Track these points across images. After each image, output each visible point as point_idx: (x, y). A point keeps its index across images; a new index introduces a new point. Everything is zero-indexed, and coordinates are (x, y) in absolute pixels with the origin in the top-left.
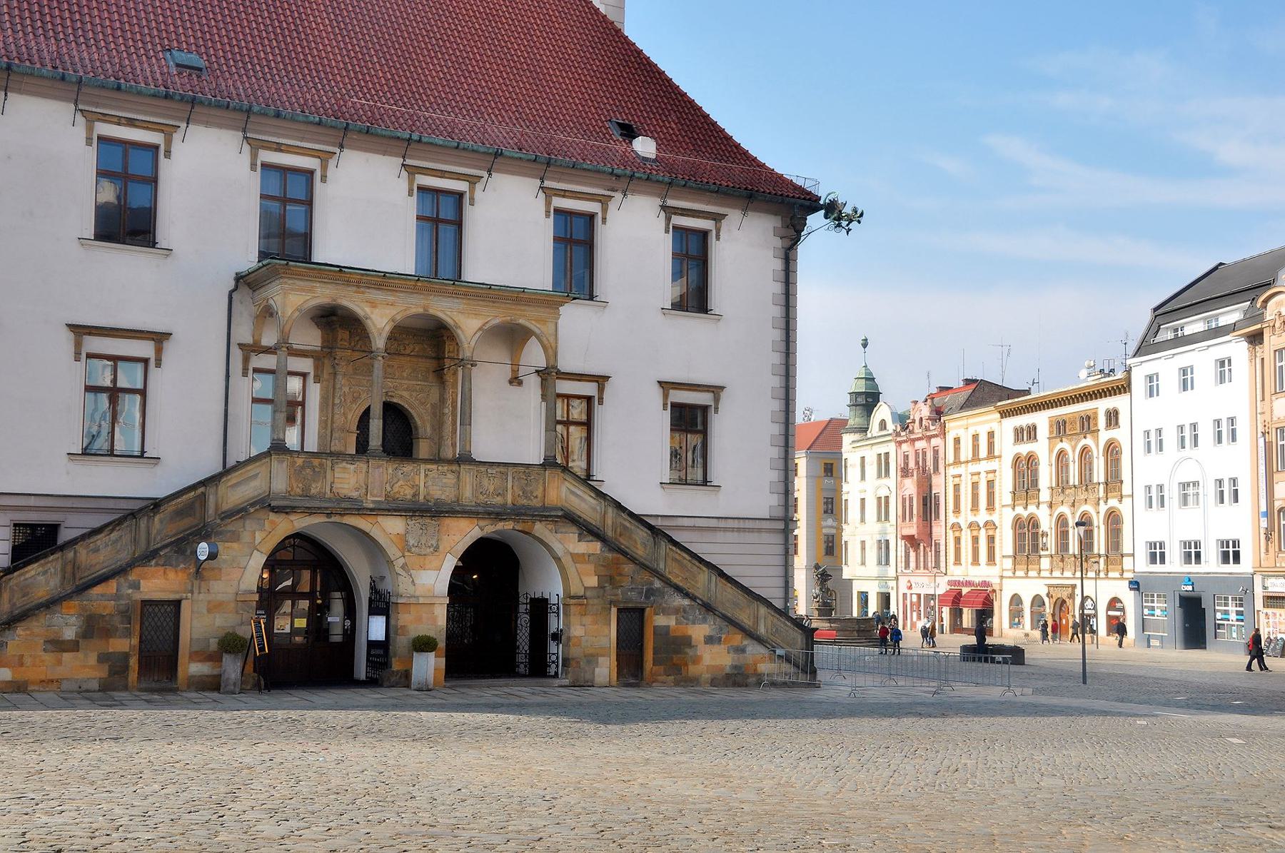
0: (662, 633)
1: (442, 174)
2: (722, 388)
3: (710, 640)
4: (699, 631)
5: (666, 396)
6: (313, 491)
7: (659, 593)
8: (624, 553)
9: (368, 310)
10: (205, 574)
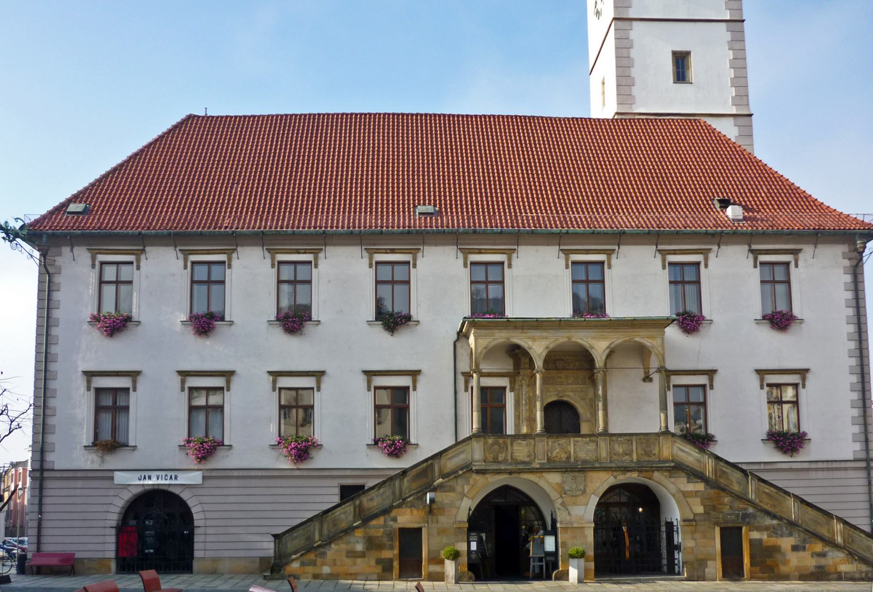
1: (587, 252)
2: (807, 370)
3: (795, 548)
4: (786, 543)
6: (500, 459)
7: (754, 516)
8: (724, 490)
9: (530, 343)
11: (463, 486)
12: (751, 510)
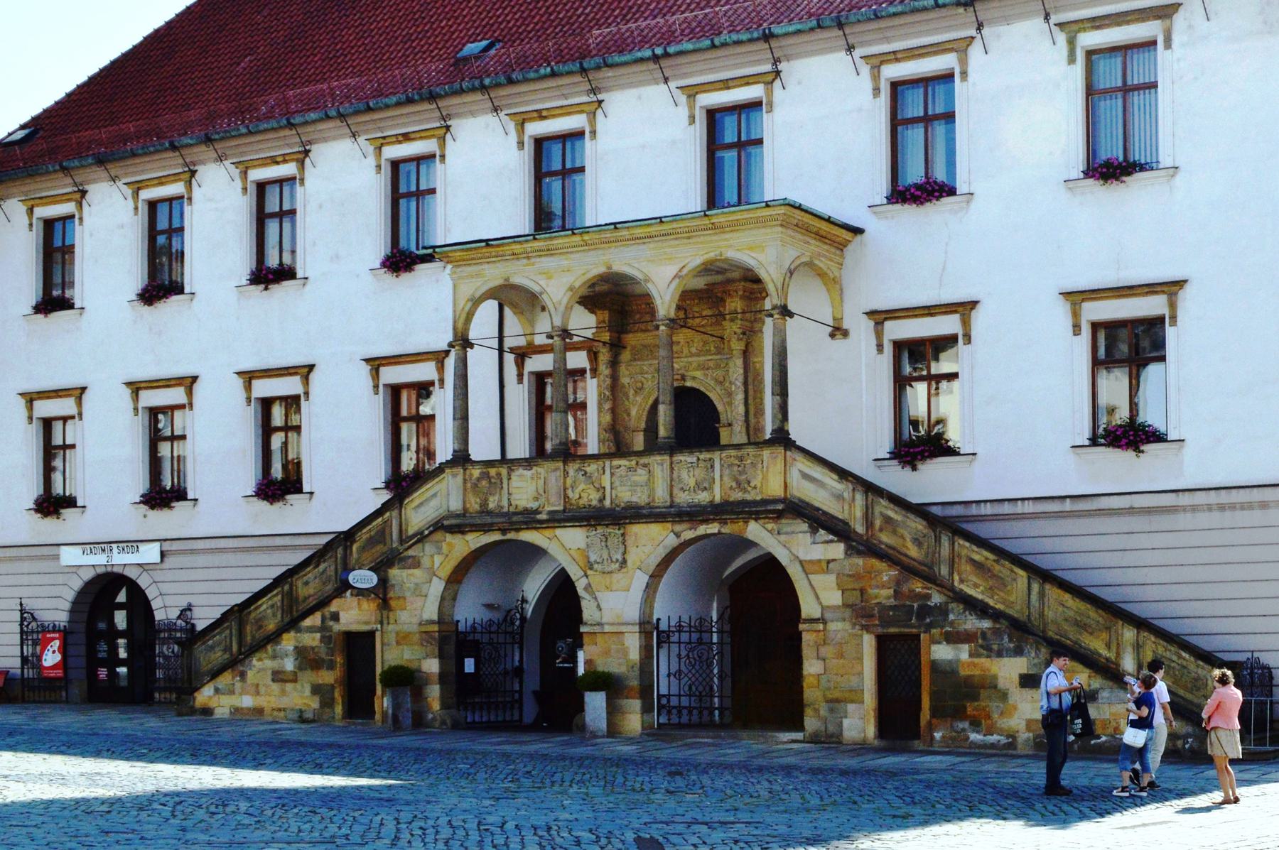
3: (1030, 681)
6: (491, 506)
10: (393, 603)
11: (432, 556)
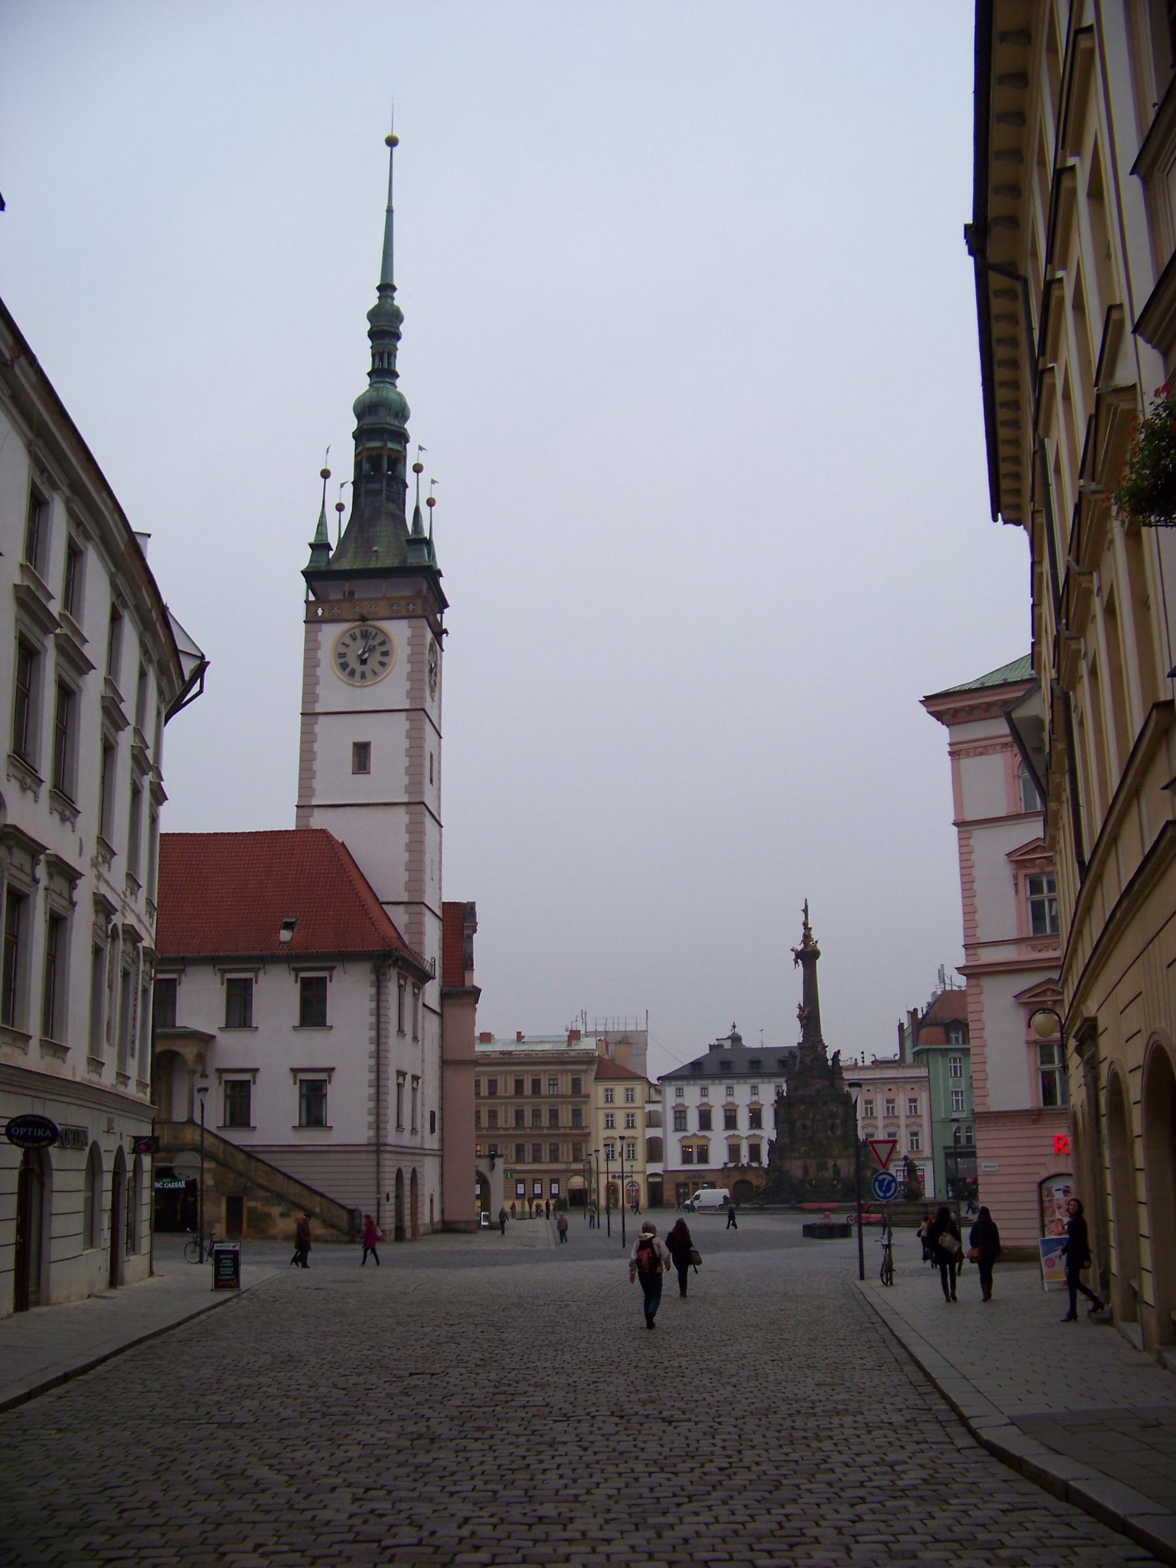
0: (252, 1211)
2: (333, 1069)
3: (282, 1215)
5: (295, 1077)
12: (249, 1184)
